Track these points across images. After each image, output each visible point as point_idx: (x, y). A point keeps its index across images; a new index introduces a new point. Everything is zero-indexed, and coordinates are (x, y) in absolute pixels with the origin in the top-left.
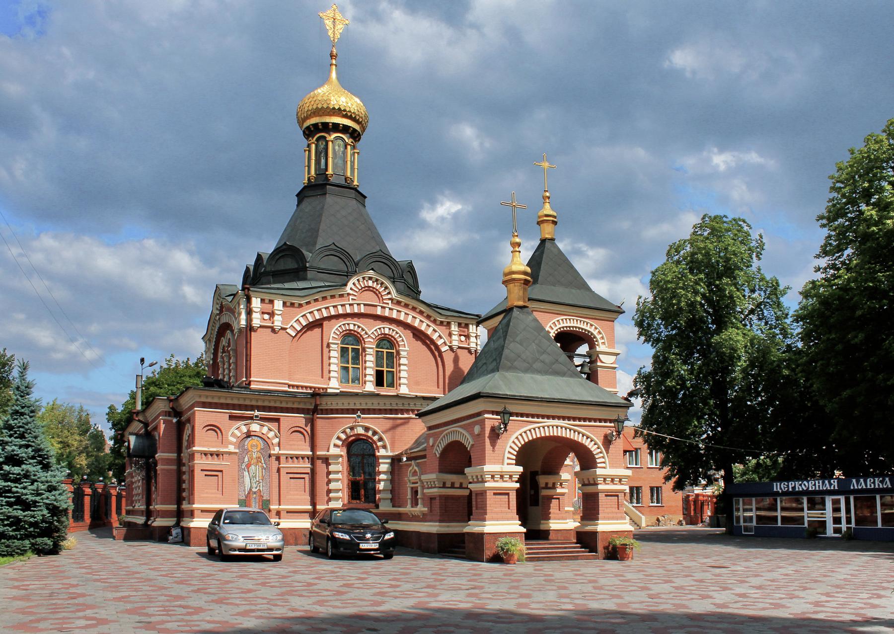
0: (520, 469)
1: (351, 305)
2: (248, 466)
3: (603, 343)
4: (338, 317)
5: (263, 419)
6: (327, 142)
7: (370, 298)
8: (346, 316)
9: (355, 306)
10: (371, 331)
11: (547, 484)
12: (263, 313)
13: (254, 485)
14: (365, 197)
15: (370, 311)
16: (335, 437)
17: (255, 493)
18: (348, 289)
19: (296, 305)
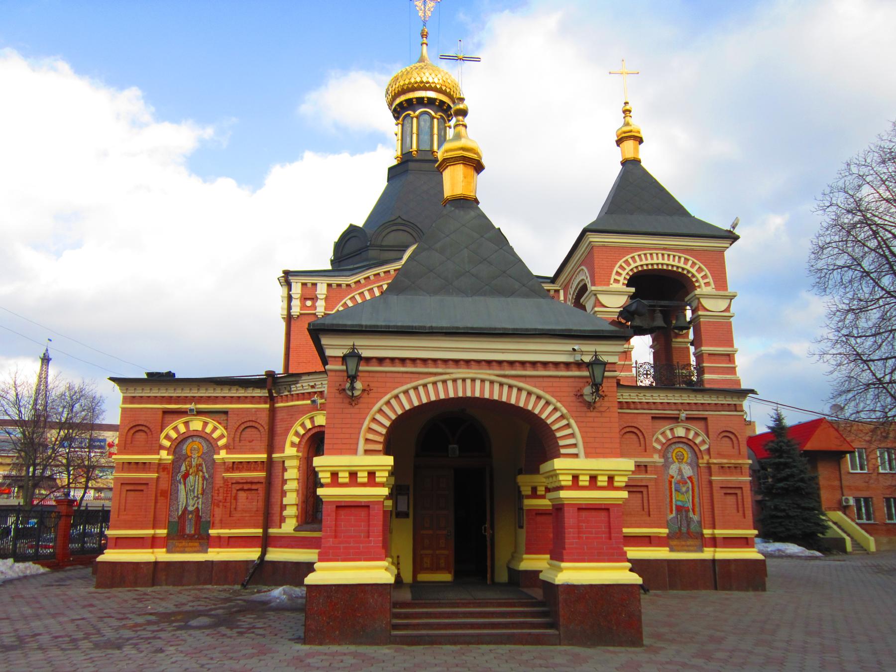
0: (389, 460)
2: (186, 476)
5: (200, 413)
11: (534, 489)
12: (306, 299)
13: (191, 502)
17: (191, 512)
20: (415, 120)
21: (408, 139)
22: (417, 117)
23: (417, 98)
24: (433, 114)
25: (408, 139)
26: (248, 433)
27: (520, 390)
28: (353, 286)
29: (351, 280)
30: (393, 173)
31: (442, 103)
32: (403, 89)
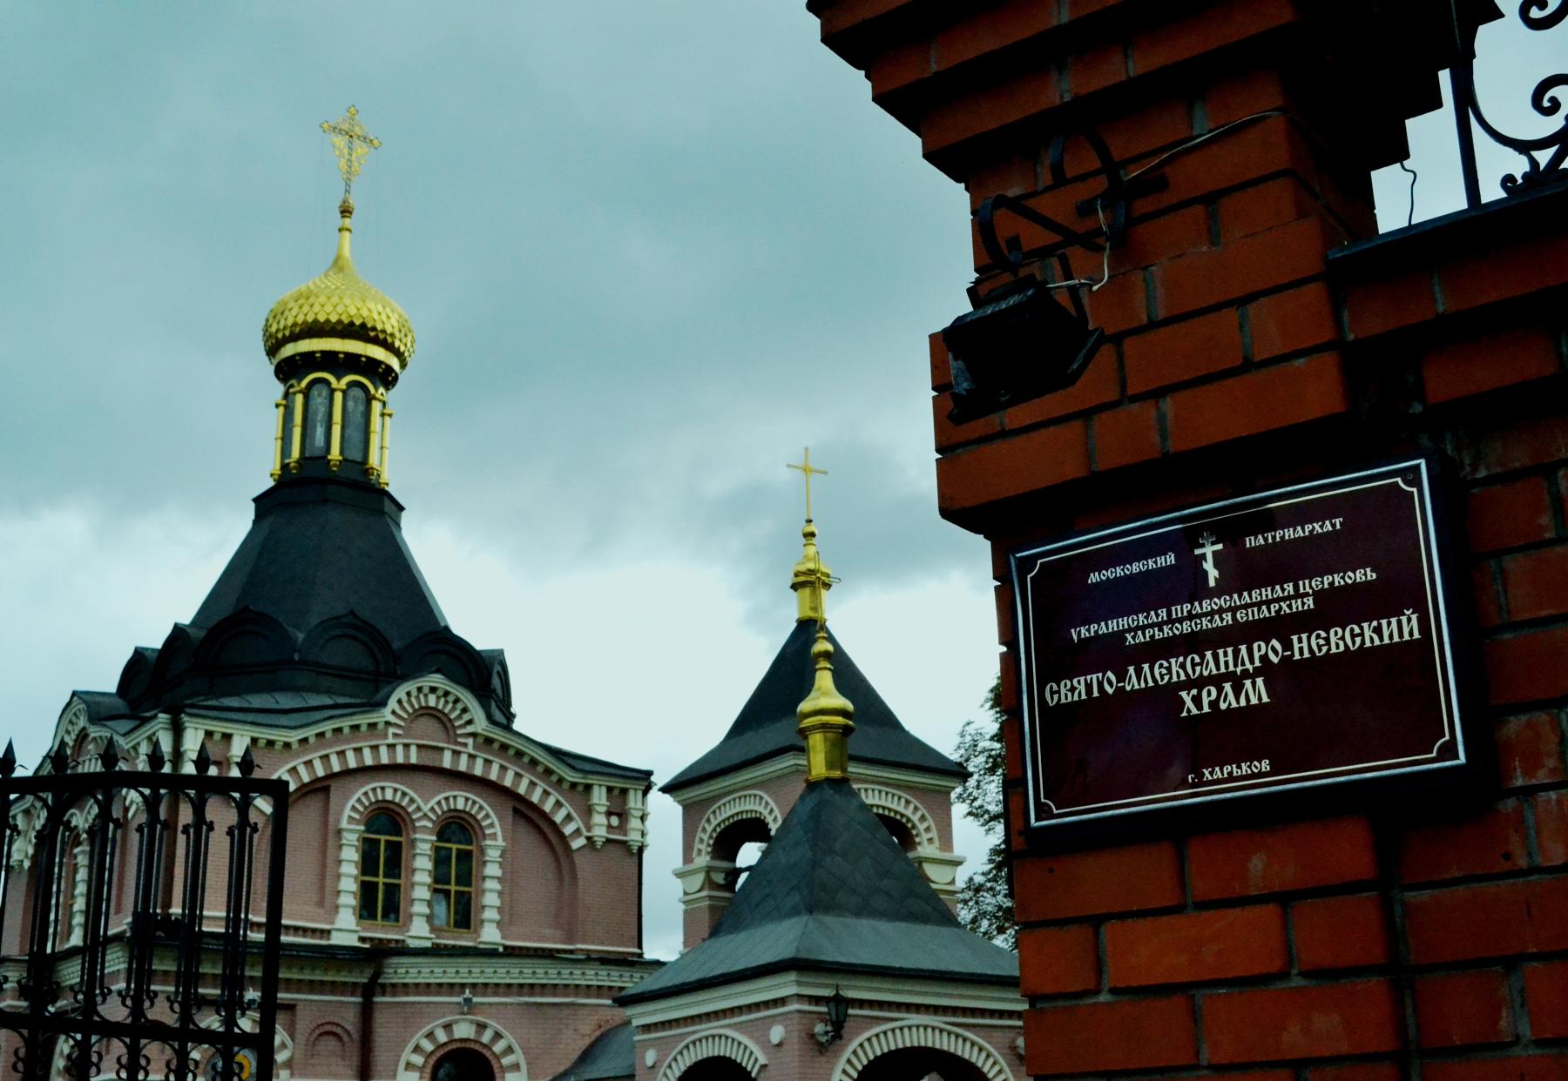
1: (391, 747)
3: (930, 840)
6: (333, 391)
7: (429, 733)
8: (378, 770)
9: (400, 749)
10: (426, 804)
14: (402, 509)
15: (429, 760)
16: (410, 1046)
18: (386, 714)
19: (278, 746)
20: (338, 396)
21: (320, 432)
22: (344, 392)
23: (347, 354)
25: (320, 432)
26: (331, 1043)
27: (965, 1040)
28: (295, 746)
29: (294, 737)
31: (389, 369)
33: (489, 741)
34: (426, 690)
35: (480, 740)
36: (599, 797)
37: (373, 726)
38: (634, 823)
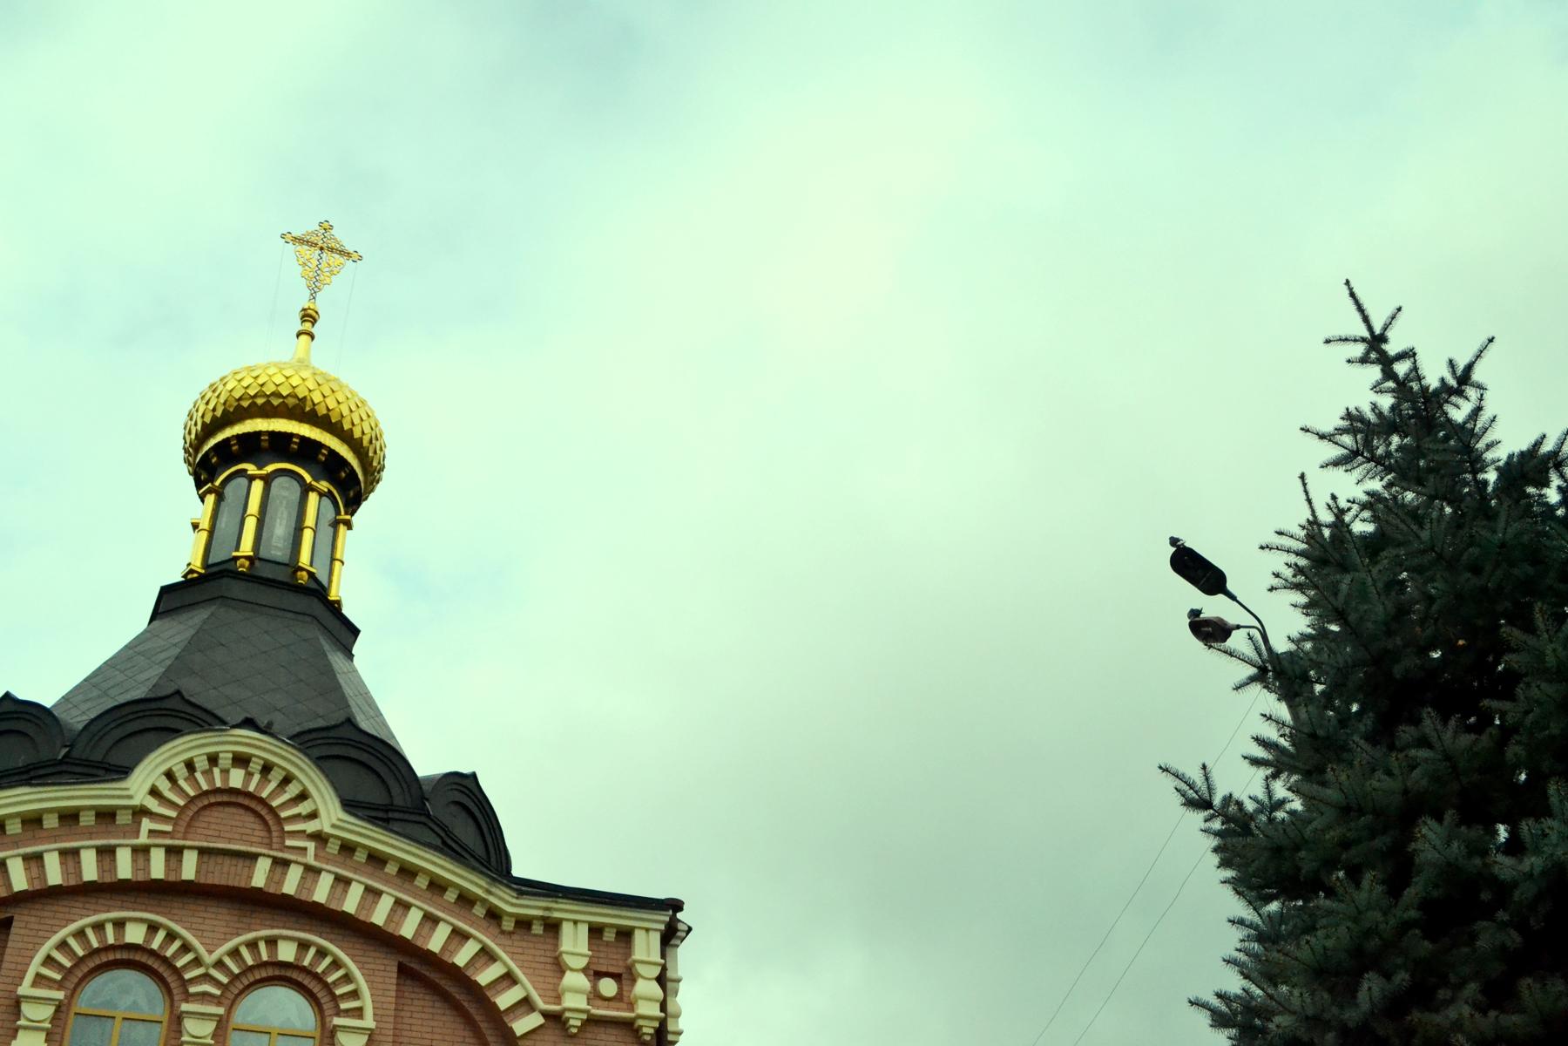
4: (79, 892)
7: (233, 832)
8: (110, 890)
14: (355, 632)
22: (268, 480)
24: (308, 479)
30: (171, 601)
32: (239, 407)
33: (348, 848)
34: (226, 759)
35: (333, 847)
36: (574, 943)
37: (106, 816)
38: (646, 988)
